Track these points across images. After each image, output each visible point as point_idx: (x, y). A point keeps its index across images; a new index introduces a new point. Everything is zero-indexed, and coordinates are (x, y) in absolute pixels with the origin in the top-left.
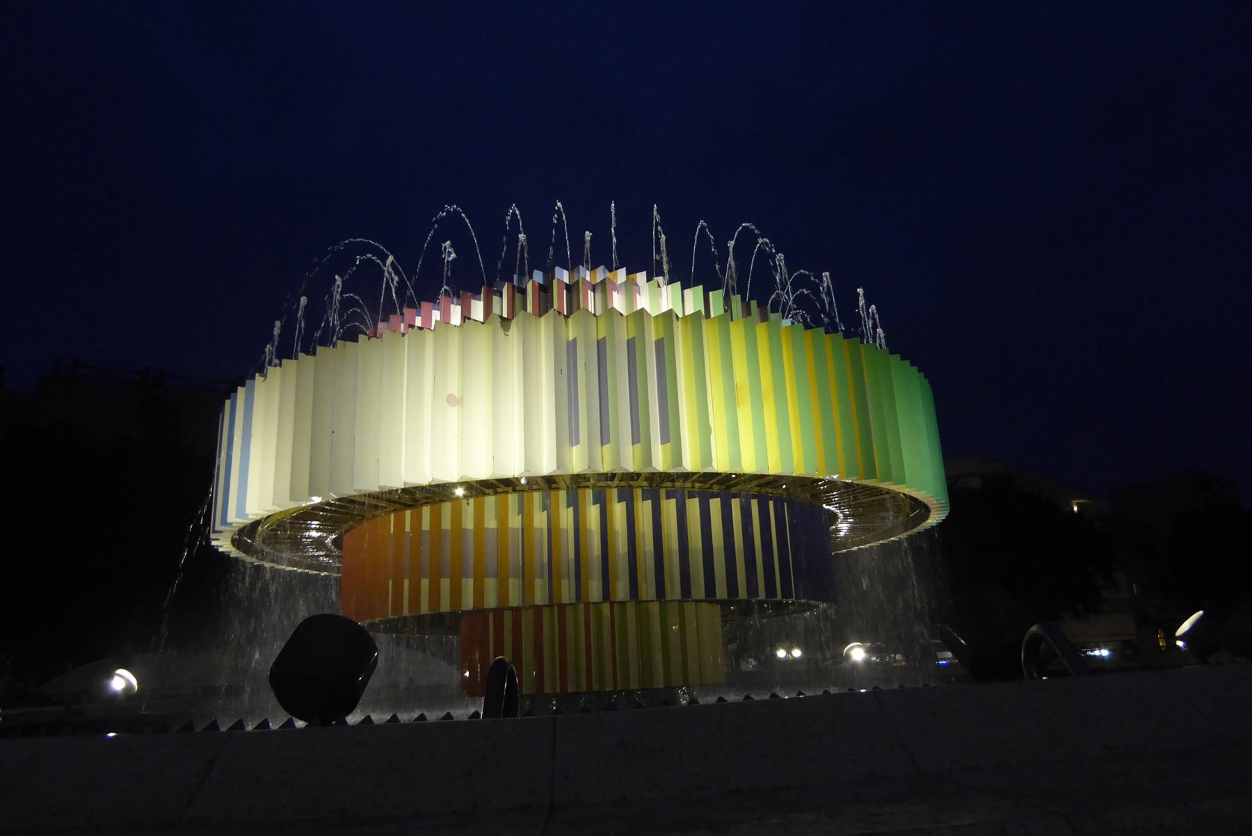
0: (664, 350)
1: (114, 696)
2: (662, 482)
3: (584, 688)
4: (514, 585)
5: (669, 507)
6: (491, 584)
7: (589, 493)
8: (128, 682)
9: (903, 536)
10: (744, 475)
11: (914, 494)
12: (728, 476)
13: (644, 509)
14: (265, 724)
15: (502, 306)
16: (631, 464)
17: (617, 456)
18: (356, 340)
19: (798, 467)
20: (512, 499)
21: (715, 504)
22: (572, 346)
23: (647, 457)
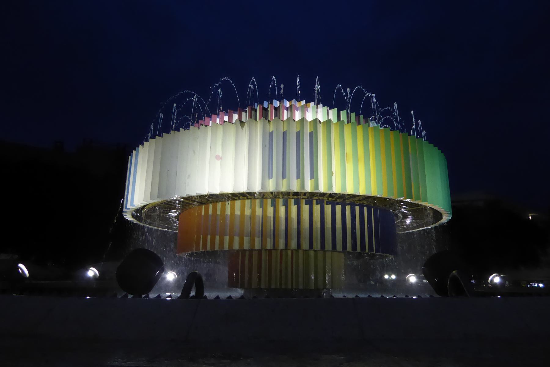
1: (89, 278)
4: (246, 239)
5: (317, 208)
6: (236, 239)
7: (281, 201)
9: (432, 226)
12: (354, 196)
15: (245, 116)
16: (295, 188)
17: (289, 185)
18: (179, 131)
19: (383, 194)
20: (247, 202)
21: (338, 208)
22: (271, 134)
23: (303, 185)
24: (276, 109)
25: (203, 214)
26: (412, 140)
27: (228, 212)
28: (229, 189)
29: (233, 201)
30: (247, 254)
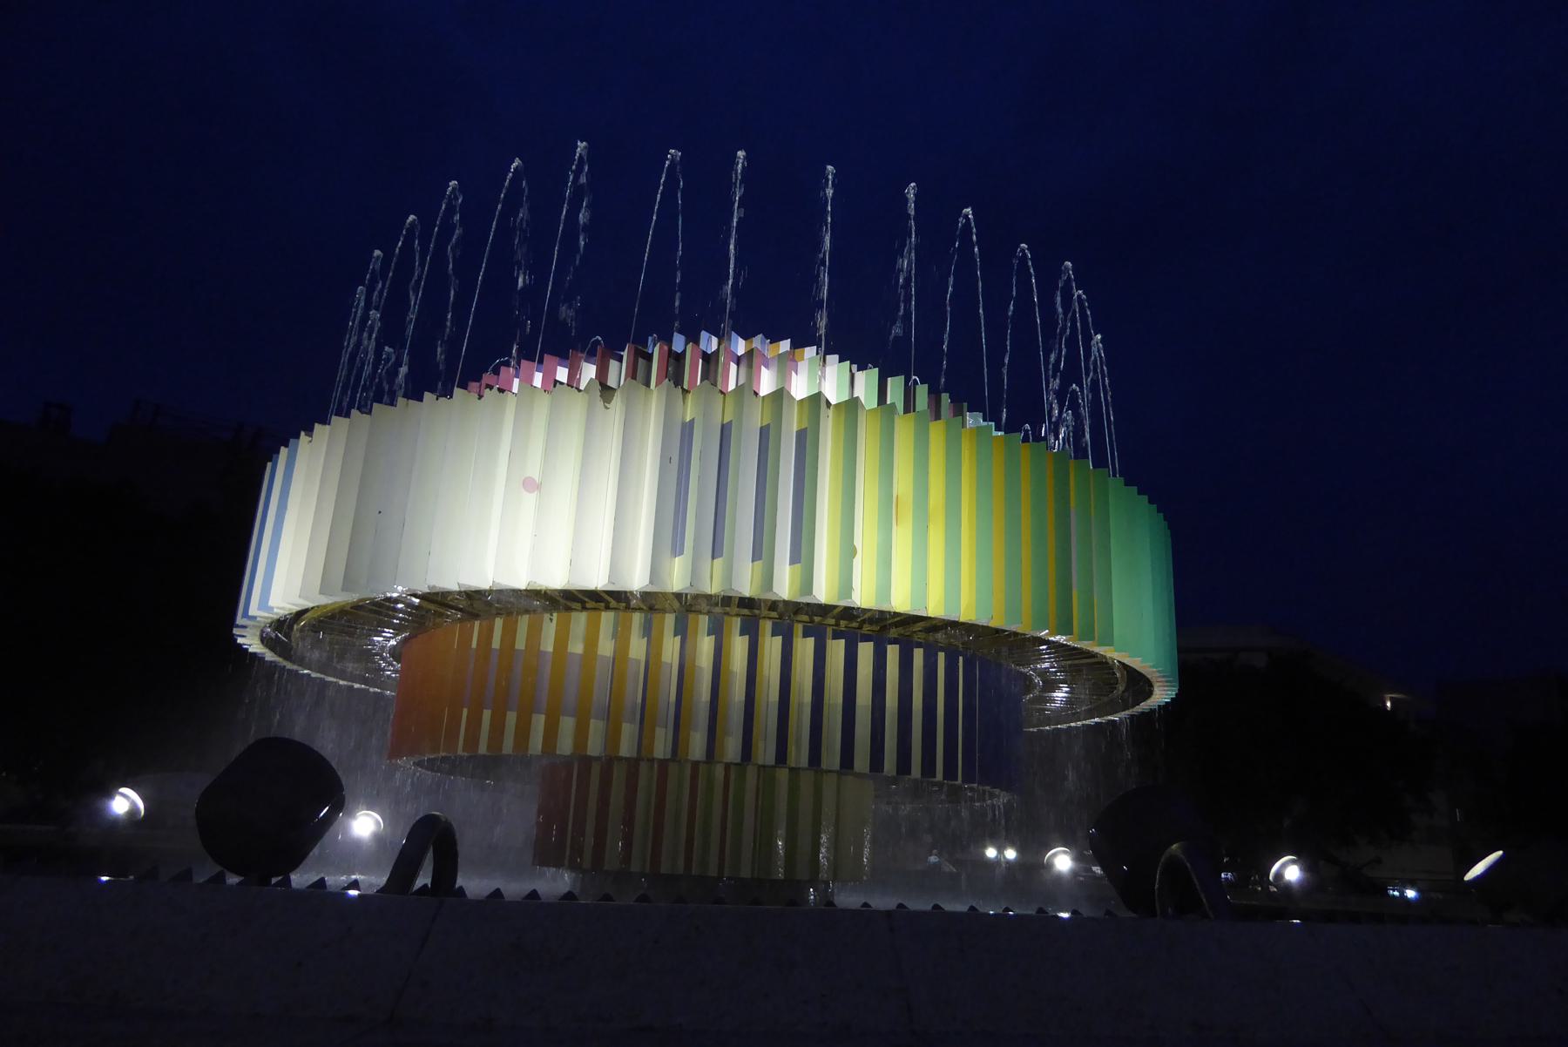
0: (806, 443)
1: (115, 823)
2: (796, 613)
3: (681, 870)
4: (596, 727)
5: (805, 648)
6: (567, 724)
7: (704, 621)
8: (134, 804)
10: (896, 614)
11: (1126, 661)
13: (772, 647)
14: (187, 876)
15: (617, 372)
18: (420, 399)
20: (607, 618)
21: (866, 651)
22: (688, 429)
24: (709, 359)
25: (474, 645)
26: (1081, 473)
27: (548, 645)
28: (556, 579)
29: (565, 614)
30: (596, 770)
